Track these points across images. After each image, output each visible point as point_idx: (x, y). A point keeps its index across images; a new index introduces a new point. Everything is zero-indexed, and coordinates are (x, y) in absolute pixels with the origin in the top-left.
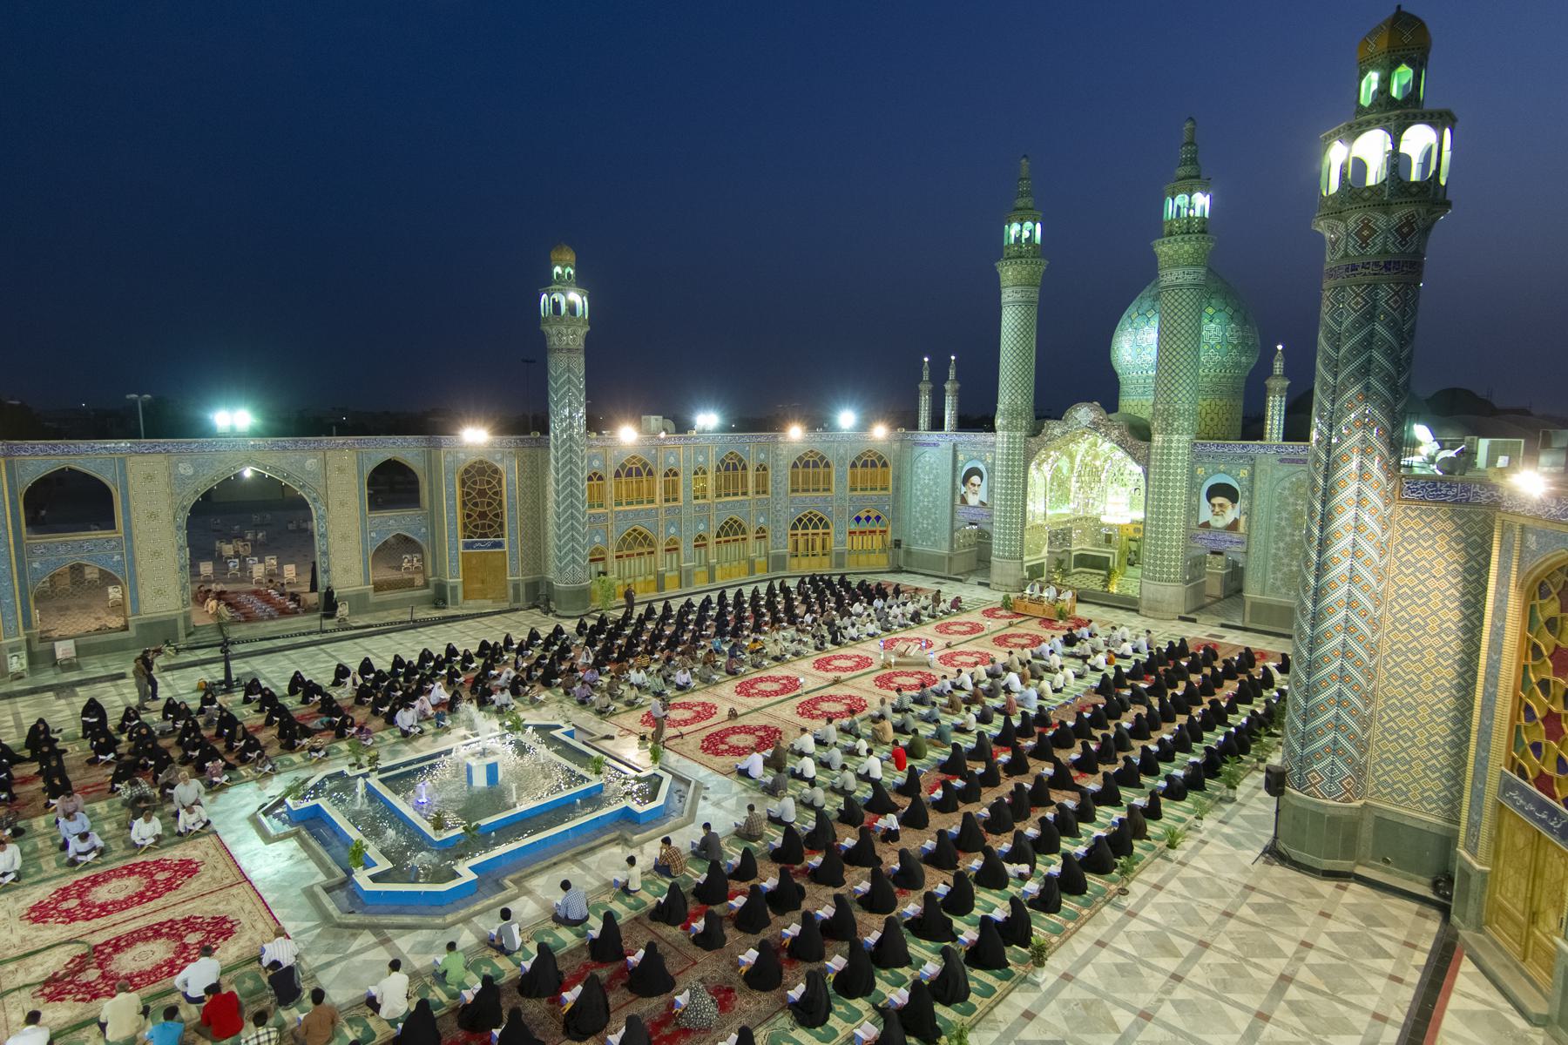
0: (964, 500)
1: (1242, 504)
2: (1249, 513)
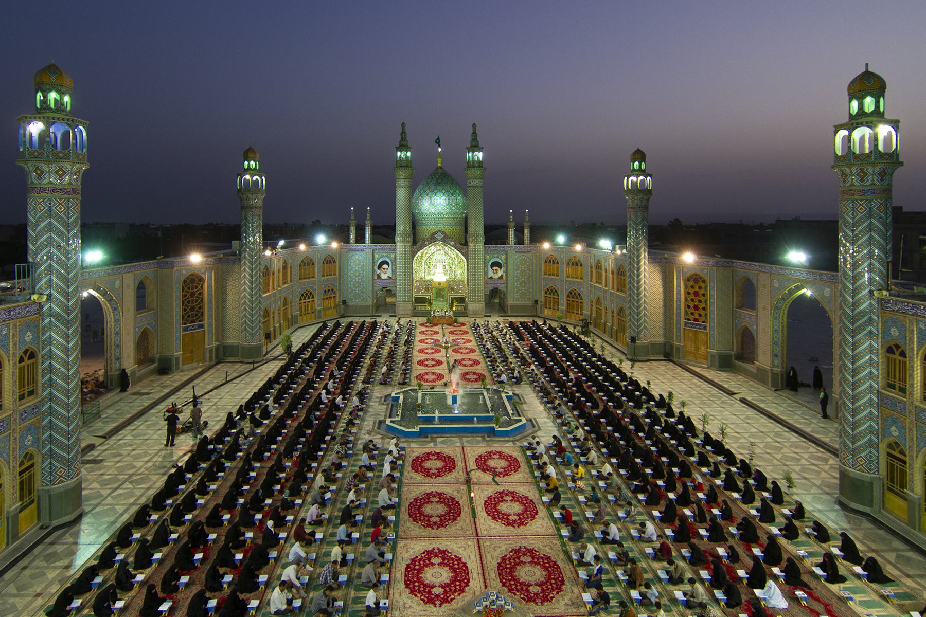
0: (379, 277)
1: (504, 269)
2: (506, 272)
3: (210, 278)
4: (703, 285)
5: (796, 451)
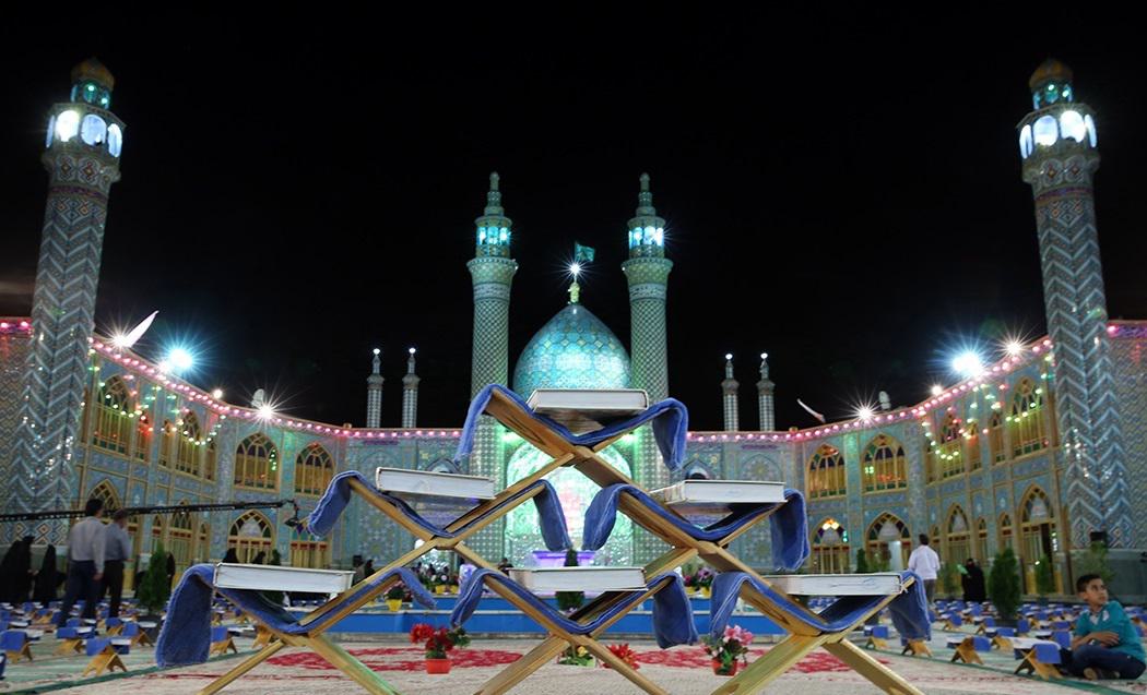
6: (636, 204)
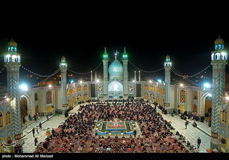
3: (53, 92)
4: (184, 93)
5: (203, 137)
6: (124, 51)
